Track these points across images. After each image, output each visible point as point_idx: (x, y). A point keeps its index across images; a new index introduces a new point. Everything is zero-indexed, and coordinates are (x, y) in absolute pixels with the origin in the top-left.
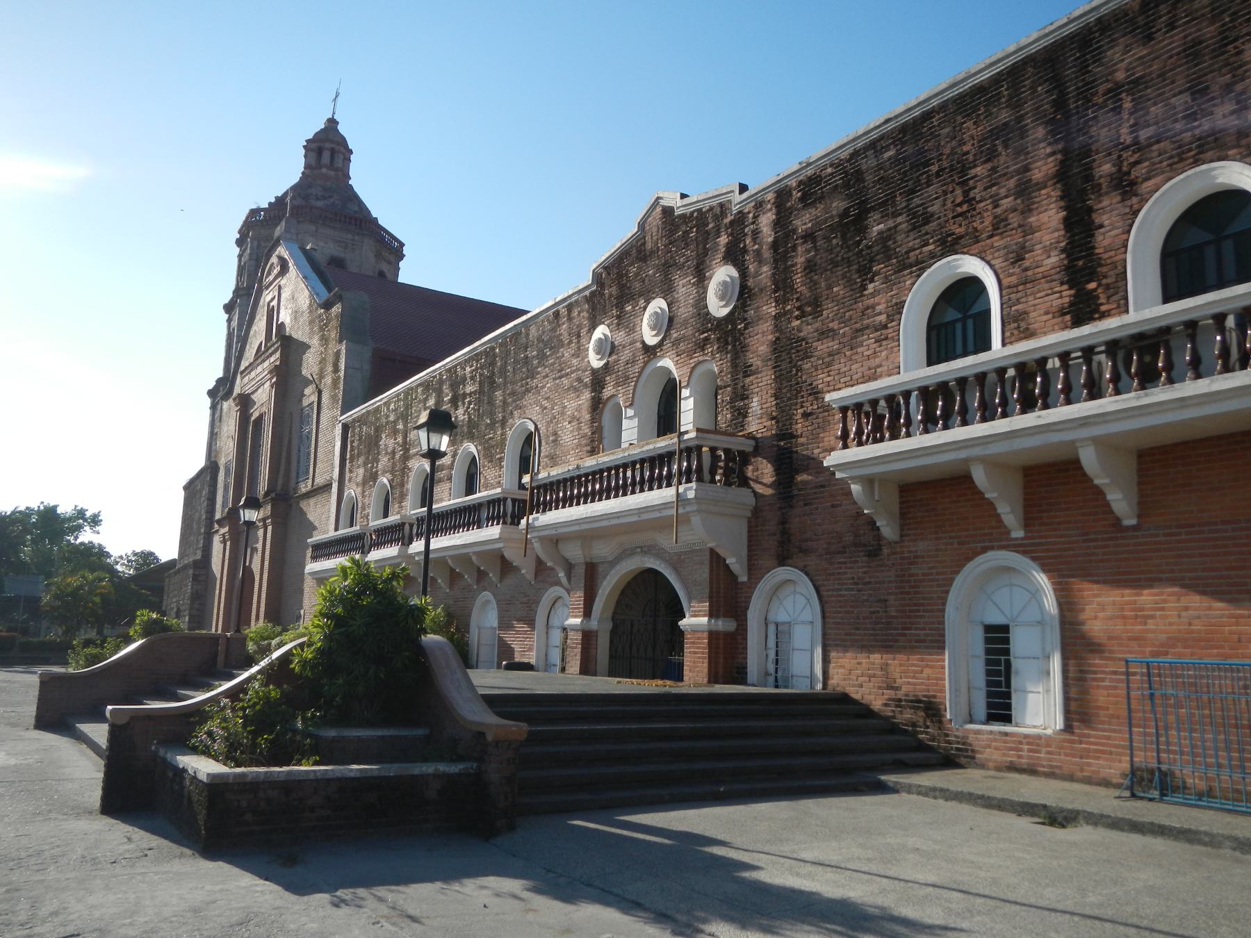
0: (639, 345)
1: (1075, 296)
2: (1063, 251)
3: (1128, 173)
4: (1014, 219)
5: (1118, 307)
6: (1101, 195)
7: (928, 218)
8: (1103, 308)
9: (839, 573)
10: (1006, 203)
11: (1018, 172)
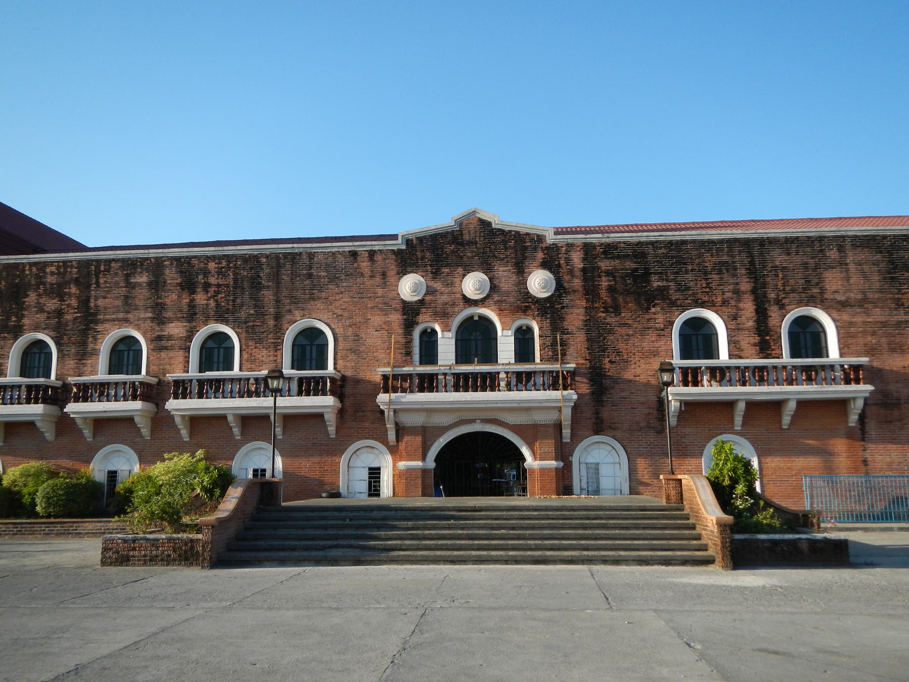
0: (459, 296)
1: (761, 340)
2: (755, 321)
3: (781, 300)
4: (733, 303)
5: (778, 348)
6: (770, 305)
7: (688, 289)
8: (772, 347)
9: (638, 440)
10: (728, 295)
11: (733, 284)
